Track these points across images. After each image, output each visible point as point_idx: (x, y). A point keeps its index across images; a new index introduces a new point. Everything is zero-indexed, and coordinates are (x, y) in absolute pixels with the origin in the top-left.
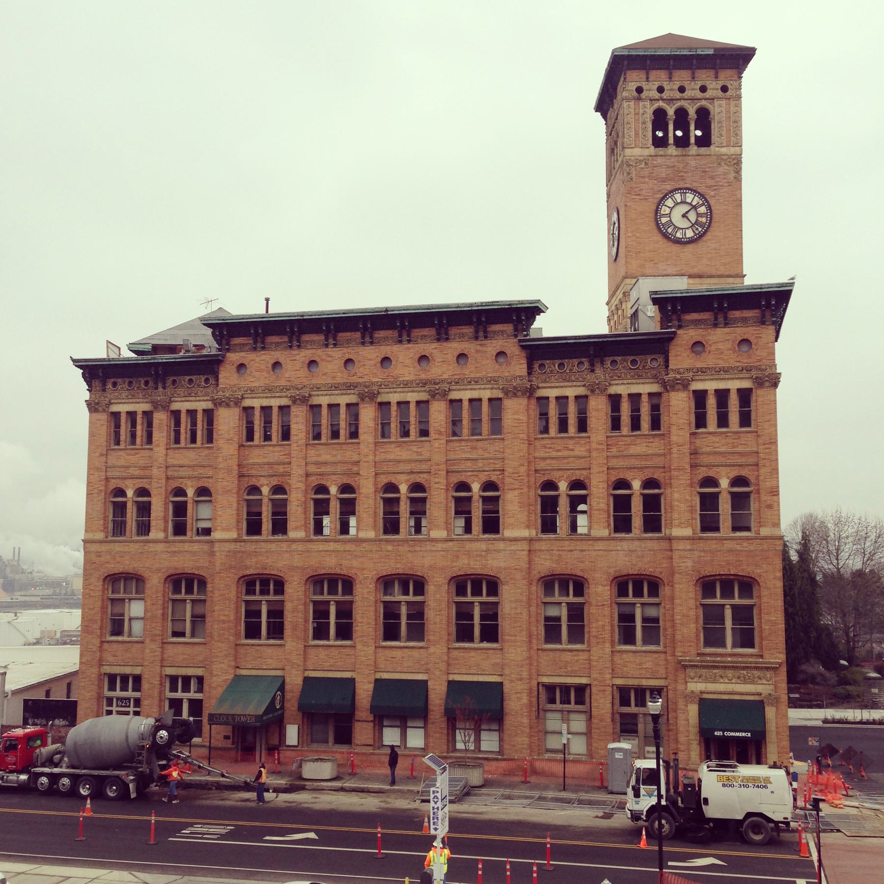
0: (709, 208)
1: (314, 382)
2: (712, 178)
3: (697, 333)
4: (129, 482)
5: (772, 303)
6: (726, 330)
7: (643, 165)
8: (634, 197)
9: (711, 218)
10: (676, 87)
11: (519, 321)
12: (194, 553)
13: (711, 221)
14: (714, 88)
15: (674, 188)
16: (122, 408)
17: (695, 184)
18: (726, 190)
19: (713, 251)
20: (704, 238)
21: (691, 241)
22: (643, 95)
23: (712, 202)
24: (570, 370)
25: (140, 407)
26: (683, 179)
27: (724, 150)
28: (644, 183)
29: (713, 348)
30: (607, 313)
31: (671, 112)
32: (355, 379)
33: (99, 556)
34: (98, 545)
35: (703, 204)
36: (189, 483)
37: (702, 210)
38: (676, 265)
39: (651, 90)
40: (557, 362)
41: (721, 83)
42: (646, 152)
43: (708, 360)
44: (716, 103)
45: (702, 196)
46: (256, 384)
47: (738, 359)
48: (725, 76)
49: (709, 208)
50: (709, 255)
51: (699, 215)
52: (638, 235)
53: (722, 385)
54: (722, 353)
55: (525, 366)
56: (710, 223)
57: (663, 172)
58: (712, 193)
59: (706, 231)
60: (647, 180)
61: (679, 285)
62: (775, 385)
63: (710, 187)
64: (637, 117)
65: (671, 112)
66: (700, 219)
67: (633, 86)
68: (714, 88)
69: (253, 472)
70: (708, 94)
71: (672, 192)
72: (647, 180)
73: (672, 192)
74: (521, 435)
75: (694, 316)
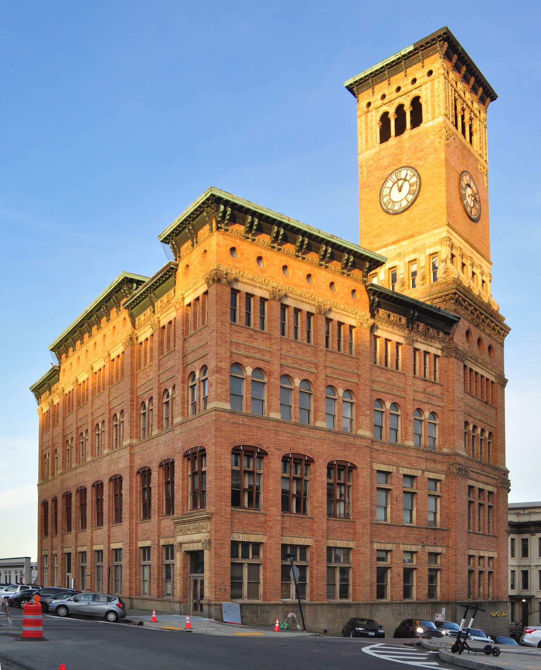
17: (409, 161)
20: (416, 203)
23: (420, 171)
26: (400, 161)
37: (414, 179)
39: (376, 100)
51: (411, 185)
57: (386, 162)
59: (417, 197)
66: (412, 188)
71: (391, 174)
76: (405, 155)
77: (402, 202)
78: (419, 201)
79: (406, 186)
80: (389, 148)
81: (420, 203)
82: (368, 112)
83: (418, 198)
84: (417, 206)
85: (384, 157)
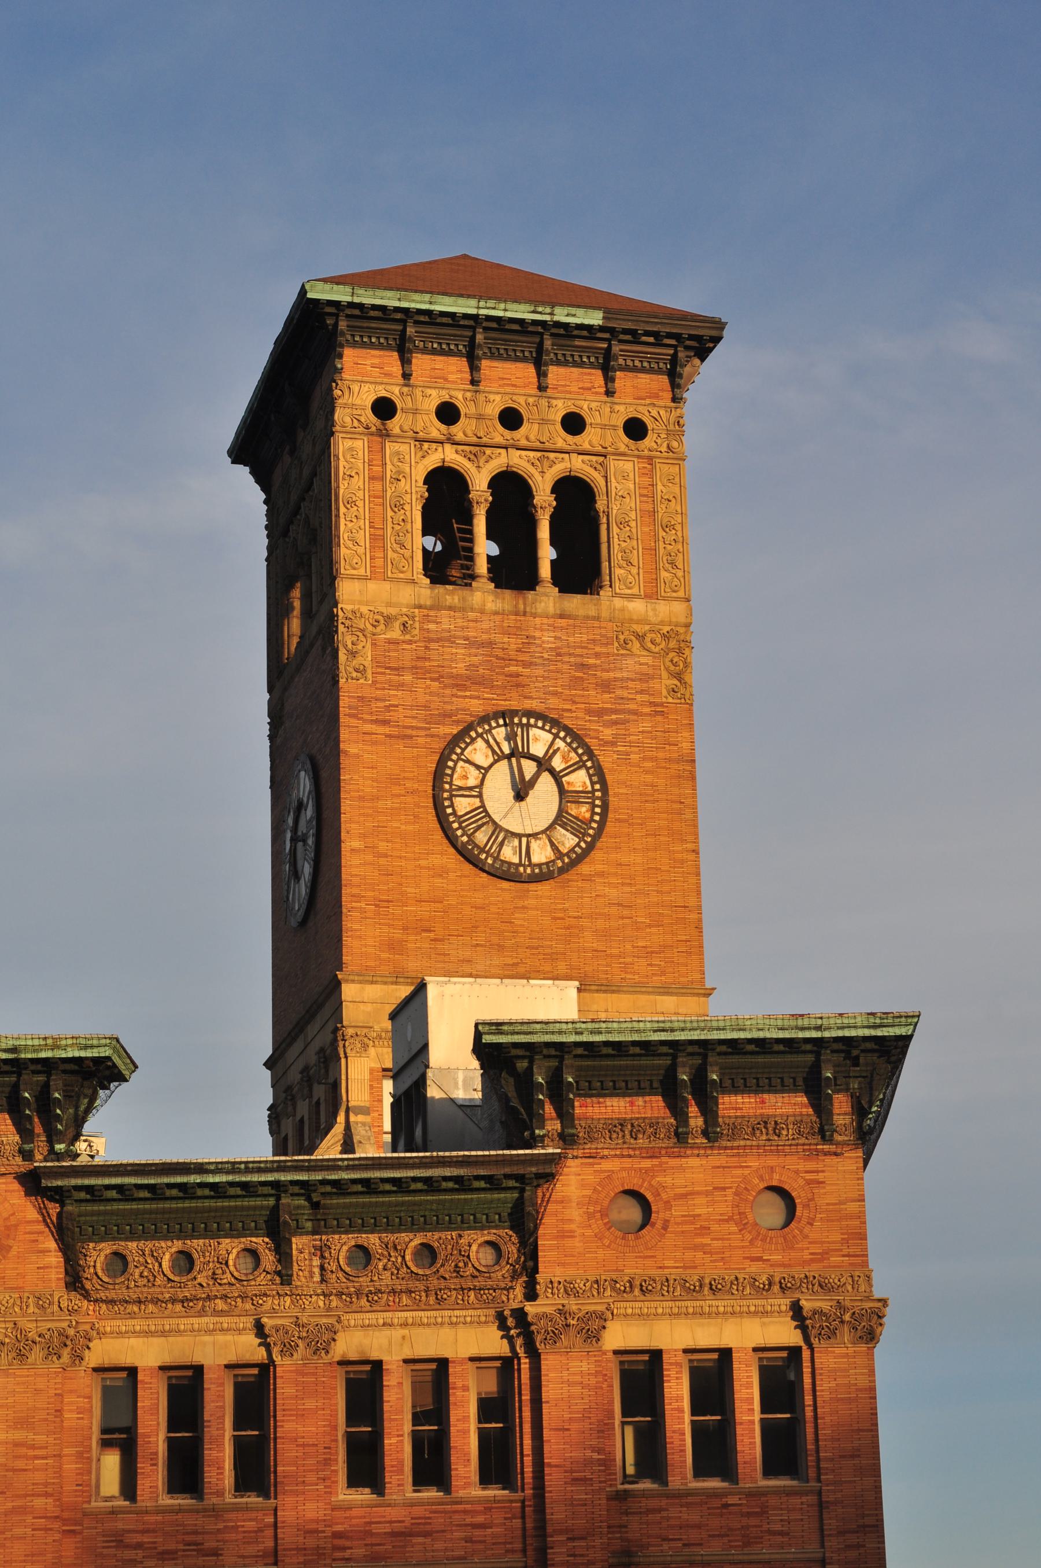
0: (599, 774)
2: (606, 686)
3: (627, 1163)
5: (848, 1075)
6: (718, 1159)
7: (395, 633)
8: (368, 727)
9: (605, 807)
10: (494, 410)
11: (44, 1105)
13: (604, 815)
14: (604, 419)
15: (490, 709)
17: (553, 702)
18: (646, 725)
19: (614, 910)
20: (584, 868)
21: (543, 875)
22: (394, 425)
23: (606, 759)
24: (214, 1277)
26: (517, 683)
27: (638, 607)
28: (400, 686)
29: (678, 1211)
30: (267, 1097)
31: (479, 483)
35: (580, 765)
37: (579, 780)
38: (501, 948)
40: (168, 1250)
41: (623, 413)
42: (406, 595)
43: (666, 1254)
44: (614, 464)
45: (576, 737)
47: (756, 1252)
48: (639, 392)
49: (599, 774)
50: (600, 924)
52: (383, 846)
53: (708, 1335)
54: (704, 1230)
55: (55, 1259)
56: (602, 824)
57: (460, 660)
58: (608, 733)
59: (591, 847)
60: (408, 678)
61: (548, 1004)
62: (871, 1337)
63: (600, 713)
64: (378, 486)
65: (479, 483)
67: (365, 396)
68: (604, 419)
70: (588, 439)
71: (485, 719)
72: (408, 678)
73: (485, 719)
74: (39, 1502)
75: (616, 1107)
76: (539, 671)
77: (535, 845)
78: (600, 867)
79: (545, 788)
80: (471, 615)
81: (601, 874)
82: (384, 434)
83: (596, 855)
84: (588, 879)
85: (451, 640)
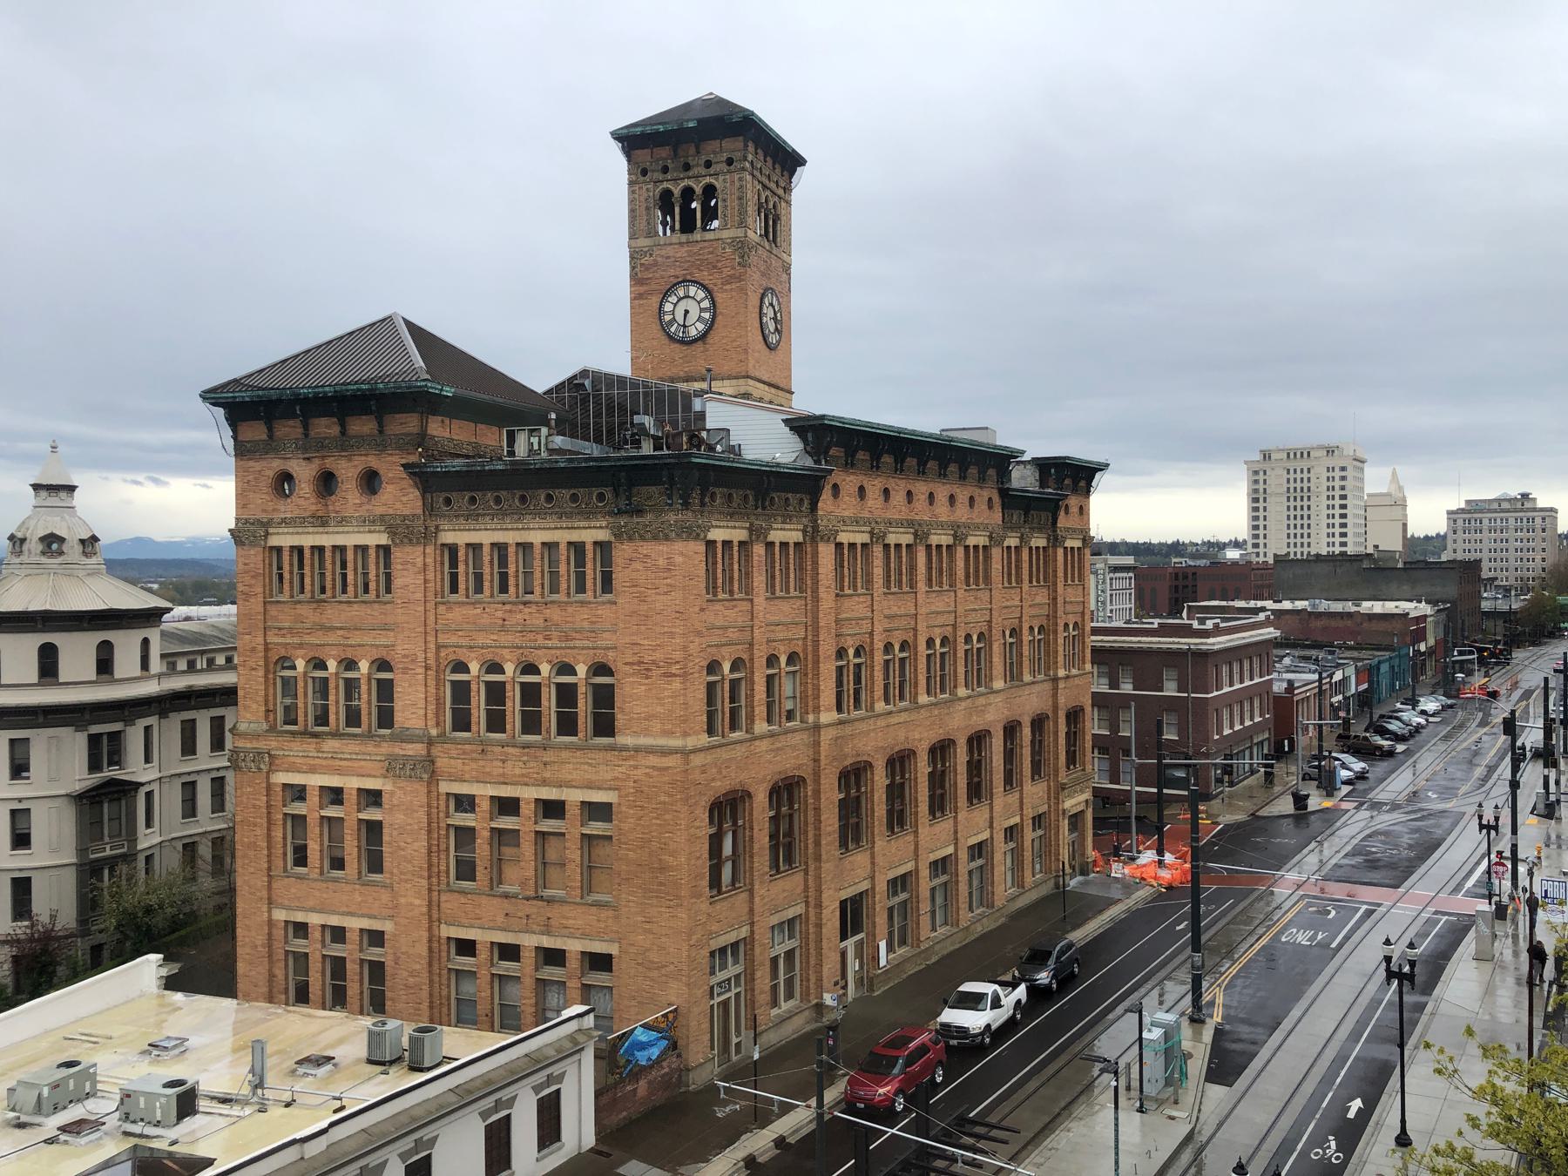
1: (889, 515)
4: (725, 651)
12: (794, 747)
16: (718, 535)
25: (738, 535)
32: (912, 516)
33: (704, 772)
34: (702, 755)
36: (782, 648)
46: (846, 513)
69: (845, 631)
